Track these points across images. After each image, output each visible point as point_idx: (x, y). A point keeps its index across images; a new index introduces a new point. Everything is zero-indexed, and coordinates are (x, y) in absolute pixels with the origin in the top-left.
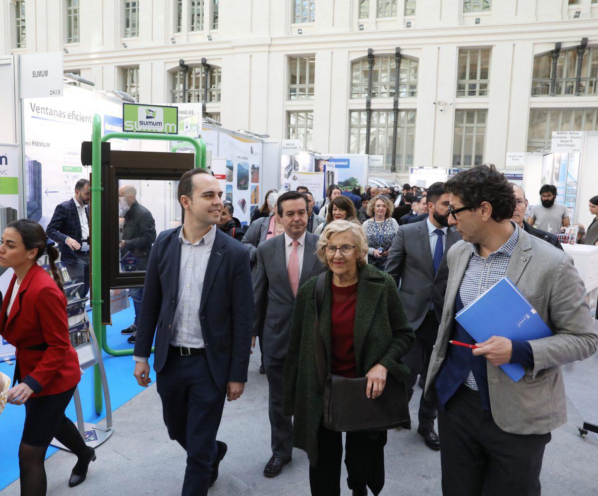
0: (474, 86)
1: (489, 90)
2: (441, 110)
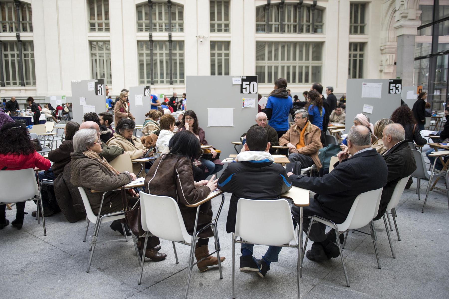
0: (219, 25)
1: (230, 29)
2: (201, 42)
